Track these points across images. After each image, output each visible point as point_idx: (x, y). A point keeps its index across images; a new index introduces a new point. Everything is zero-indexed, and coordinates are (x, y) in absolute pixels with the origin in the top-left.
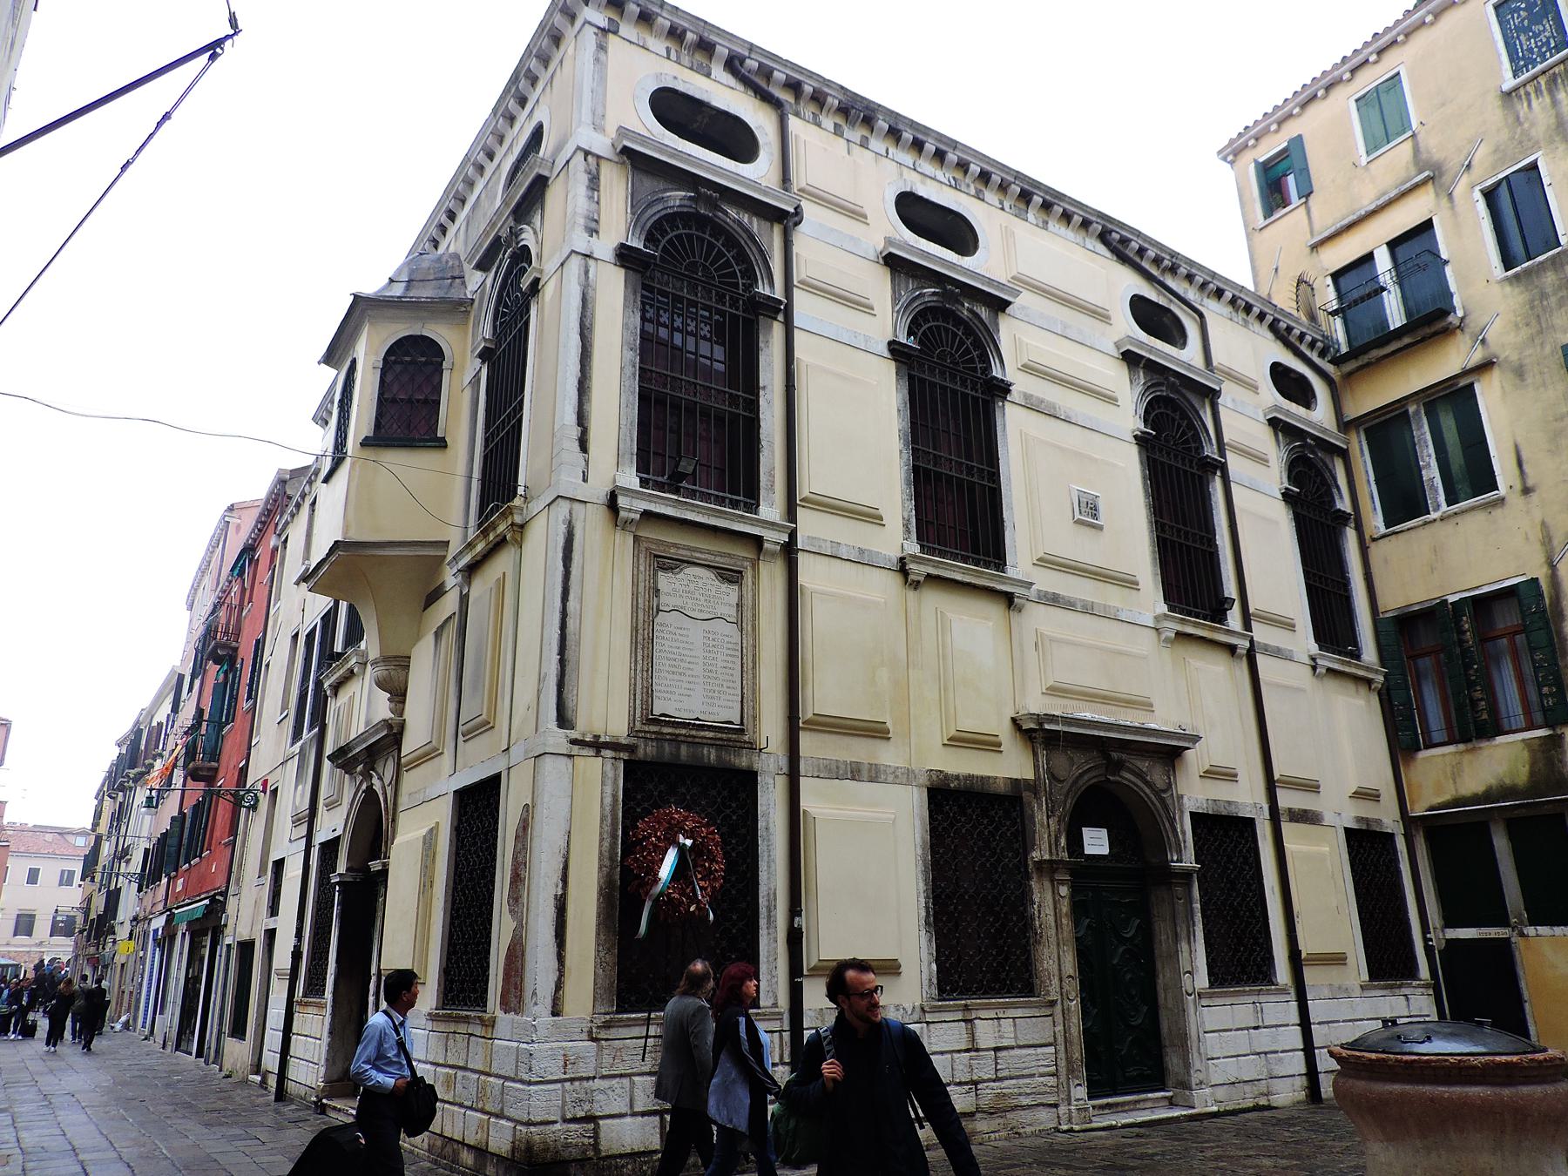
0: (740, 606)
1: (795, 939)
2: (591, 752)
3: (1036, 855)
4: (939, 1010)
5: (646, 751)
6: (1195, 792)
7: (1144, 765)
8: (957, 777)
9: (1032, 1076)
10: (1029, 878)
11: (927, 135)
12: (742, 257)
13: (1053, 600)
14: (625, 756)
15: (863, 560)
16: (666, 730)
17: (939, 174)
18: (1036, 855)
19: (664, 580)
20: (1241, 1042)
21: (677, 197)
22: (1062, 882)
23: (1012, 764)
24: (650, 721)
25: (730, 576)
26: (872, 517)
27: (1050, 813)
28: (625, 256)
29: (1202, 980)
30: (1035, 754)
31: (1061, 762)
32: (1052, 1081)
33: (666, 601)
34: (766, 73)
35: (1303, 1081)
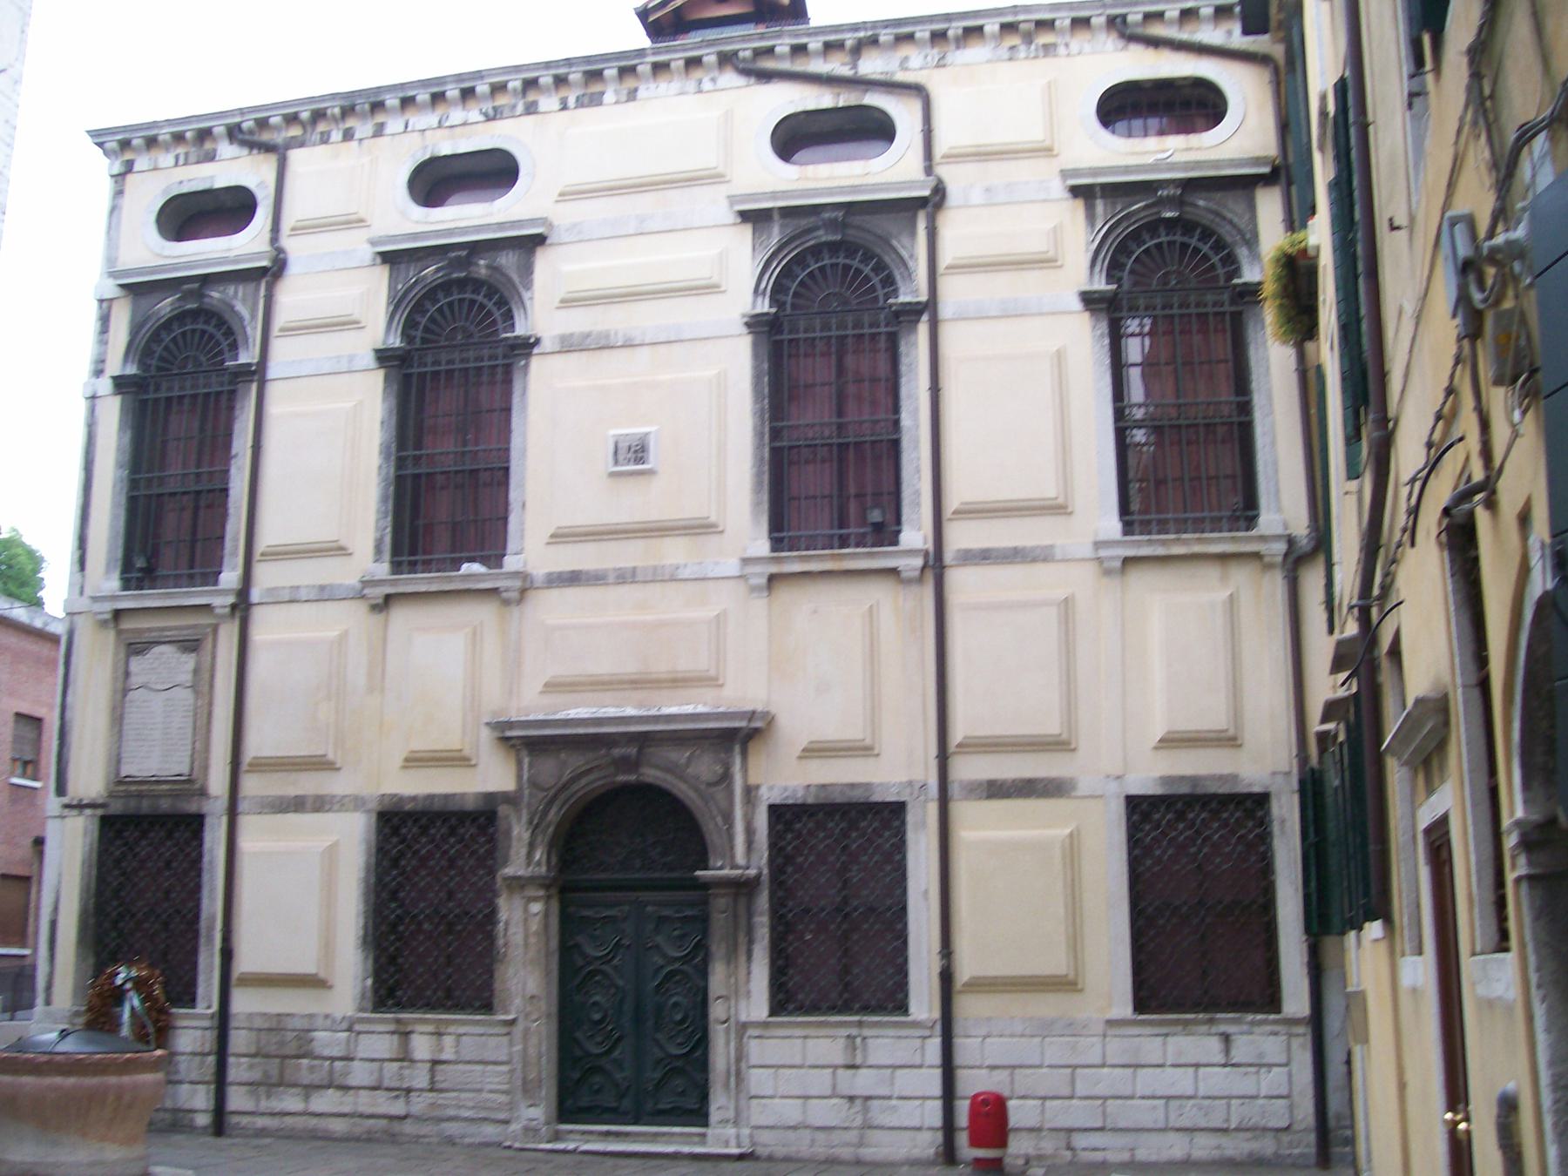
0: (196, 671)
1: (227, 954)
2: (75, 812)
3: (509, 871)
4: (368, 1021)
5: (117, 808)
6: (782, 776)
7: (680, 756)
8: (414, 798)
9: (480, 1091)
10: (496, 894)
11: (445, 83)
12: (230, 332)
13: (573, 579)
14: (100, 812)
15: (325, 595)
16: (133, 788)
17: (474, 115)
18: (509, 871)
19: (136, 664)
20: (820, 1081)
21: (166, 306)
22: (535, 899)
23: (494, 775)
24: (120, 783)
25: (191, 645)
26: (339, 550)
27: (535, 829)
28: (120, 383)
29: (757, 1005)
30: (519, 763)
31: (550, 770)
32: (503, 1098)
33: (135, 680)
34: (263, 124)
35: (939, 1136)
